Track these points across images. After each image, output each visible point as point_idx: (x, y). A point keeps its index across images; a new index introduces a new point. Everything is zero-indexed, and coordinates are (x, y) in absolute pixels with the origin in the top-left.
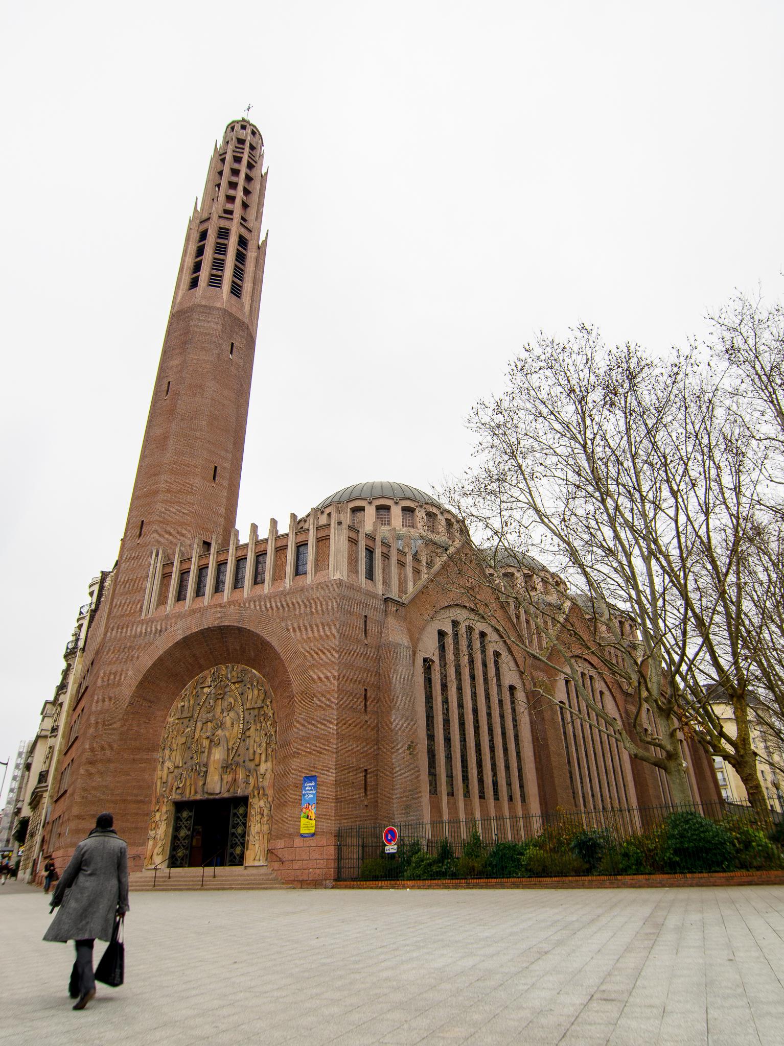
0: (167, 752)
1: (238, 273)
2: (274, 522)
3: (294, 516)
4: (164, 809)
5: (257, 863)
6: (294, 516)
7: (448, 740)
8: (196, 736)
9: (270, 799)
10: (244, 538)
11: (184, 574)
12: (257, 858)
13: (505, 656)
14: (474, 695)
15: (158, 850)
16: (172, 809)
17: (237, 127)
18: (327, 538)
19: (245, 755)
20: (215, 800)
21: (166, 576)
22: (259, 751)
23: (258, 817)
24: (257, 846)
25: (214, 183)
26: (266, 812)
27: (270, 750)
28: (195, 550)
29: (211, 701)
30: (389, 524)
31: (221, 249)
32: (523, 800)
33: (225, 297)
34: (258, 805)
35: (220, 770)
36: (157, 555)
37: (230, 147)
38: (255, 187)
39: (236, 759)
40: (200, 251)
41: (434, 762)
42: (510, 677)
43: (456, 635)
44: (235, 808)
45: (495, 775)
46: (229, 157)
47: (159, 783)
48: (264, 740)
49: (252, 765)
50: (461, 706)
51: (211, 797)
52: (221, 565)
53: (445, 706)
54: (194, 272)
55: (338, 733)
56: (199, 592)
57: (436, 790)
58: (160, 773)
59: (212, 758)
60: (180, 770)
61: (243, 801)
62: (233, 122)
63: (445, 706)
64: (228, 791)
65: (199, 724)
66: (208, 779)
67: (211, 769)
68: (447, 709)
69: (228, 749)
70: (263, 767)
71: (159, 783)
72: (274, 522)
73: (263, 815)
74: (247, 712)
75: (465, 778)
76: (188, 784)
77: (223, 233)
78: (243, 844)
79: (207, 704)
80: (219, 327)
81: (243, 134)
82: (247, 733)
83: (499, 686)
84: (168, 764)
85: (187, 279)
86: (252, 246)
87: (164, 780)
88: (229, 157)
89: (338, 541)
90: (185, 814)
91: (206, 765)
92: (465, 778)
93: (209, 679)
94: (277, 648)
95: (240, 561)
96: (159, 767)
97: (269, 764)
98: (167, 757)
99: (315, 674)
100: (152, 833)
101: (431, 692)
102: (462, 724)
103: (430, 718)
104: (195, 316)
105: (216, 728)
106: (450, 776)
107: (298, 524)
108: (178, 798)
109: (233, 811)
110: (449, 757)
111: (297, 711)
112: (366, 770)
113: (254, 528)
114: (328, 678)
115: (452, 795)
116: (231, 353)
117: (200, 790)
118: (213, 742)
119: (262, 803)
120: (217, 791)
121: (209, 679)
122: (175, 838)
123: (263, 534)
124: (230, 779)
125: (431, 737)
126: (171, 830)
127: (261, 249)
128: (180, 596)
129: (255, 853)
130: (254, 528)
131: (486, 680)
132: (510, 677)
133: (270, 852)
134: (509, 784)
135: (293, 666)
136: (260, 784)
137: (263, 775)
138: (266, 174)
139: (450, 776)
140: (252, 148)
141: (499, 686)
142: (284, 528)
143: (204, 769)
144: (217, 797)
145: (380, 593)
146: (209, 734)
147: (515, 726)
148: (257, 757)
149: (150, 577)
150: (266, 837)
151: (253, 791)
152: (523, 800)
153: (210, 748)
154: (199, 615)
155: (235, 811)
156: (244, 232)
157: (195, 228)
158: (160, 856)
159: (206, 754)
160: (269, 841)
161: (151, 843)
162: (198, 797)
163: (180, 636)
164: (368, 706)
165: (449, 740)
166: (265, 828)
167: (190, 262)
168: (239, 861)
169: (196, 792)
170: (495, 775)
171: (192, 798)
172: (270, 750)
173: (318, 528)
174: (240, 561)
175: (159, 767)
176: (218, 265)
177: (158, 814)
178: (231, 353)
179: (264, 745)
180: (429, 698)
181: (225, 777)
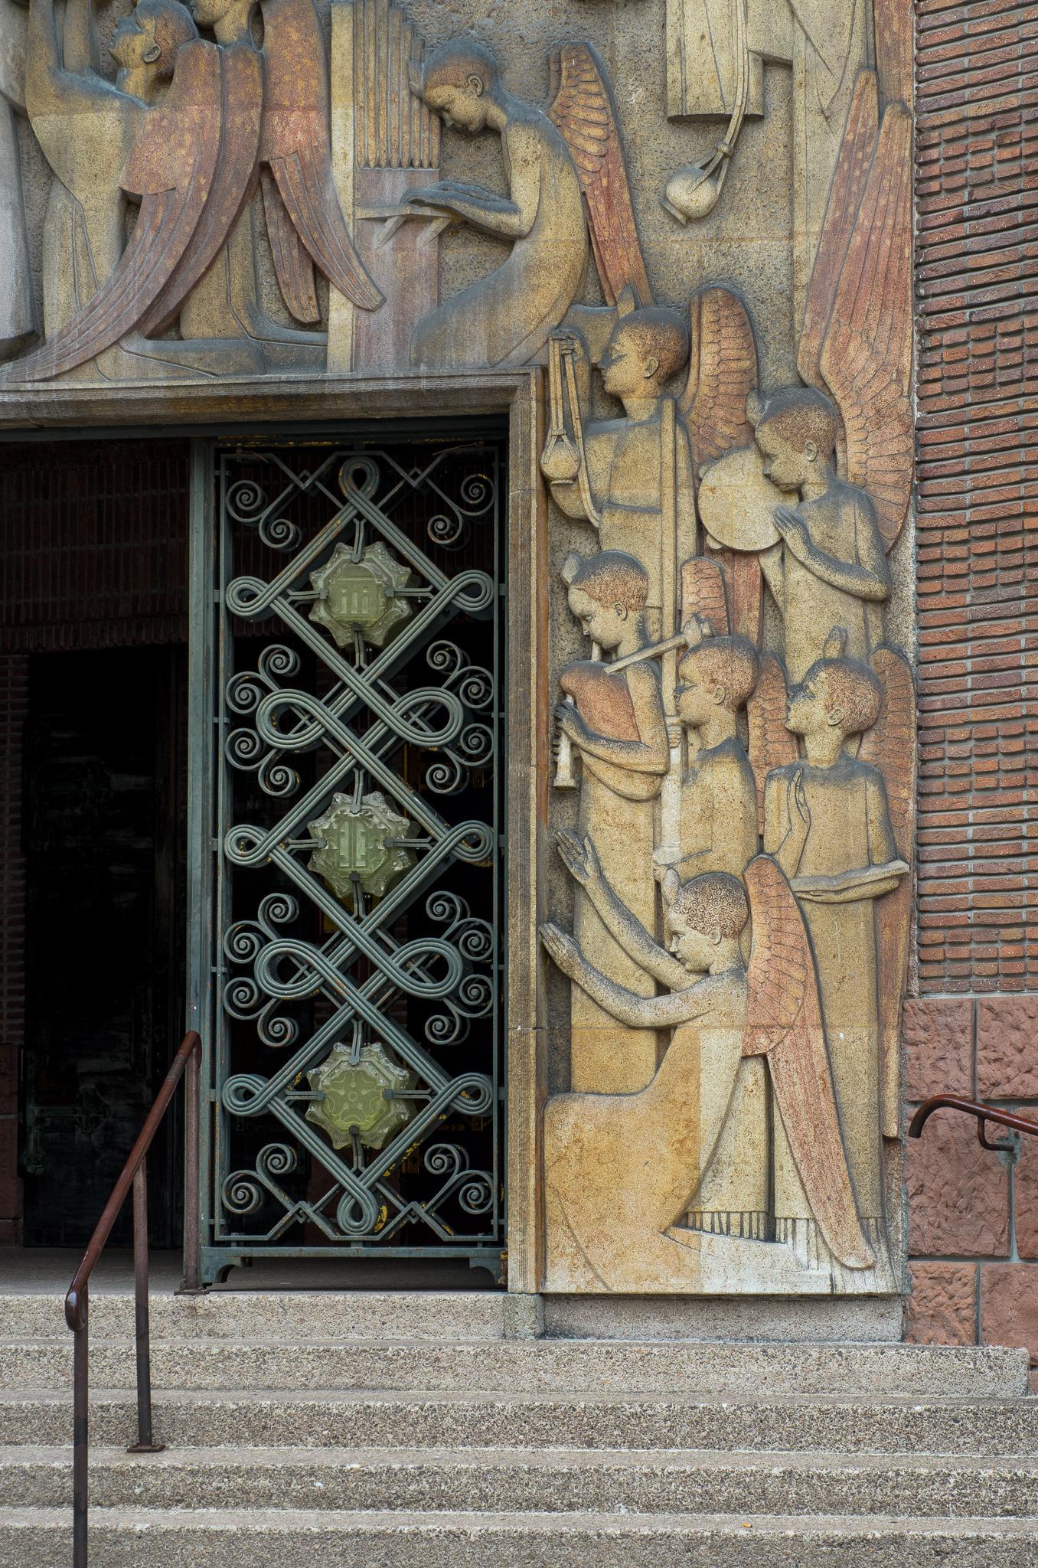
5: (727, 1266)
9: (873, 452)
12: (733, 1194)
23: (705, 685)
24: (716, 1048)
34: (650, 531)
44: (253, 558)
64: (164, 322)
73: (767, 659)
109: (212, 594)
119: (741, 502)
150: (845, 940)
151: (565, 332)
155: (269, 595)
166: (831, 828)
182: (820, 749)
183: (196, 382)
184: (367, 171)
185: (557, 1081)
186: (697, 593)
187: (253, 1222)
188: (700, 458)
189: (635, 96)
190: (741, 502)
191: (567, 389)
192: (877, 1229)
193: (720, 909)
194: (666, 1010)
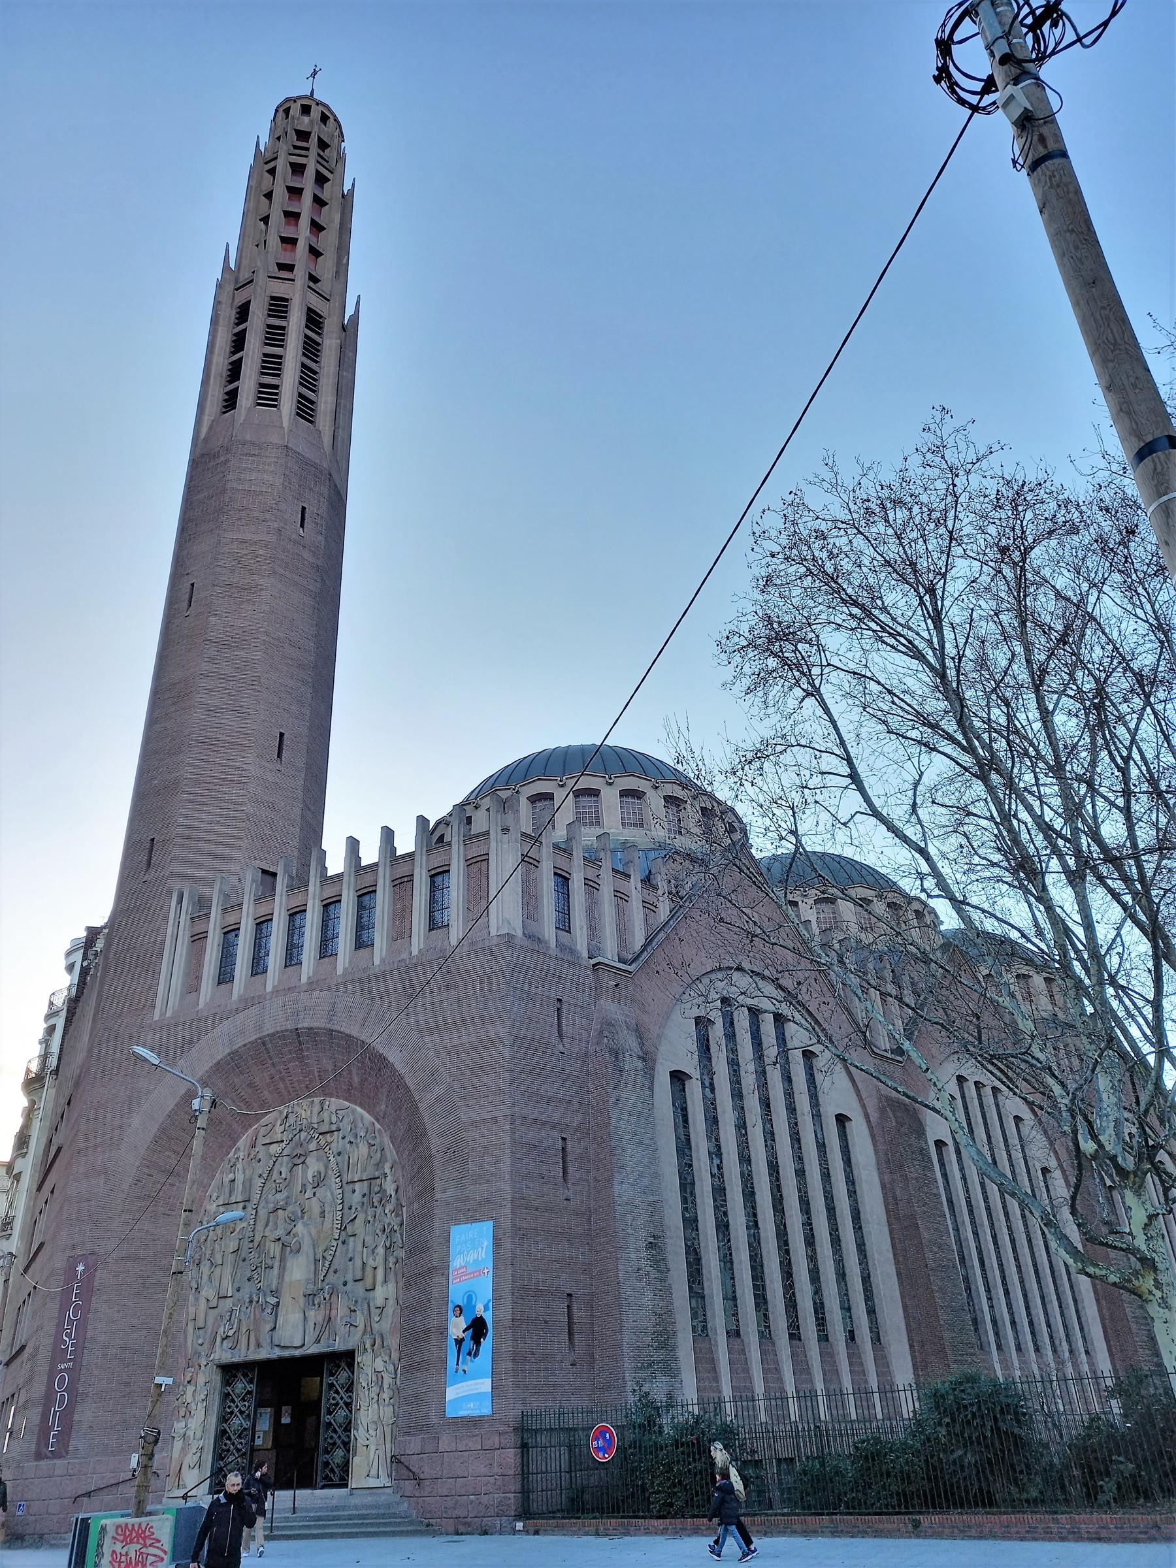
0: (205, 1268)
1: (308, 377)
2: (388, 835)
3: (422, 821)
4: (201, 1380)
6: (422, 821)
7: (723, 1227)
8: (258, 1239)
9: (395, 1355)
10: (336, 864)
11: (230, 932)
12: (373, 1472)
13: (824, 1058)
14: (770, 1137)
15: (191, 1459)
16: (217, 1378)
17: (296, 110)
18: (485, 858)
19: (346, 1270)
20: (293, 1360)
21: (199, 938)
22: (371, 1263)
23: (375, 1389)
24: (372, 1448)
25: (257, 218)
26: (387, 1380)
27: (392, 1260)
28: (247, 890)
29: (283, 1170)
30: (598, 823)
31: (276, 336)
32: (876, 1339)
33: (285, 424)
34: (373, 1368)
35: (302, 1300)
36: (180, 902)
37: (284, 148)
38: (330, 217)
39: (331, 1277)
40: (239, 342)
41: (699, 1272)
42: (838, 1095)
43: (730, 1023)
44: (332, 1375)
45: (817, 1291)
46: (282, 165)
47: (190, 1329)
48: (382, 1240)
49: (359, 1289)
50: (745, 1159)
51: (286, 1353)
52: (296, 914)
53: (716, 1161)
54: (230, 382)
55: (514, 1225)
56: (258, 966)
57: (705, 1328)
58: (192, 1310)
59: (287, 1279)
60: (229, 1302)
61: (347, 1358)
62: (287, 100)
63: (716, 1161)
64: (318, 1341)
65: (263, 1213)
66: (280, 1320)
67: (286, 1300)
68: (720, 1167)
69: (316, 1261)
70: (380, 1294)
71: (190, 1329)
72: (388, 835)
74: (346, 1187)
75: (761, 1299)
76: (244, 1329)
77: (279, 306)
78: (346, 1445)
79: (275, 1175)
80: (278, 481)
81: (304, 123)
82: (349, 1229)
83: (817, 1116)
84: (208, 1292)
85: (217, 394)
86: (330, 326)
87: (201, 1324)
88: (282, 165)
89: (504, 860)
90: (240, 1386)
91: (276, 1293)
92: (761, 1299)
93: (279, 1129)
94: (399, 1066)
95: (330, 905)
96: (191, 1298)
97: (391, 1286)
98: (205, 1278)
99: (466, 1115)
100: (179, 1426)
101: (688, 1136)
102: (749, 1195)
103: (687, 1186)
104: (234, 463)
105: (293, 1220)
106: (732, 1298)
107: (432, 835)
108: (227, 1357)
110: (727, 1260)
111: (438, 1185)
112: (570, 1295)
113: (353, 845)
114: (493, 1121)
115: (738, 1333)
116: (302, 525)
117: (265, 1339)
118: (288, 1247)
120: (298, 1343)
121: (279, 1129)
122: (222, 1434)
123: (370, 854)
124: (320, 1318)
125: (691, 1222)
126: (213, 1420)
127: (349, 331)
128: (225, 976)
129: (369, 1464)
130: (353, 845)
131: (792, 1109)
132: (838, 1095)
133: (396, 1460)
134: (847, 1309)
135: (430, 1098)
136: (376, 1326)
137: (382, 1309)
138: (352, 191)
139: (732, 1298)
140: (323, 145)
141: (817, 1116)
142: (405, 843)
143: (273, 1301)
144: (297, 1353)
145: (585, 954)
146: (280, 1232)
147: (852, 1193)
148: (369, 1271)
149: (168, 942)
150: (388, 1430)
152: (876, 1339)
153: (283, 1259)
154: (254, 1010)
156: (316, 303)
157: (225, 298)
158: (196, 1471)
159: (276, 1271)
160: (394, 1438)
161: (178, 1445)
162: (264, 1354)
163: (221, 1053)
164: (570, 1169)
165: (727, 1226)
166: (387, 1413)
167: (222, 362)
168: (340, 1478)
169: (259, 1345)
170: (817, 1291)
171: (252, 1357)
172: (392, 1260)
173: (468, 839)
174: (330, 905)
175: (191, 1298)
176: (272, 365)
177: (190, 1389)
178: (302, 525)
179: (381, 1251)
180: (684, 1146)
181: (311, 1314)
182: (387, 1400)
183: (322, 1350)
184: (341, 1319)
185: (355, 1454)
186: (374, 1378)
187: (326, 1478)
188: (375, 1357)
189: (371, 1305)
190: (379, 1364)
191: (361, 1349)
192: (390, 1476)
193: (374, 1427)
194: (367, 1443)
